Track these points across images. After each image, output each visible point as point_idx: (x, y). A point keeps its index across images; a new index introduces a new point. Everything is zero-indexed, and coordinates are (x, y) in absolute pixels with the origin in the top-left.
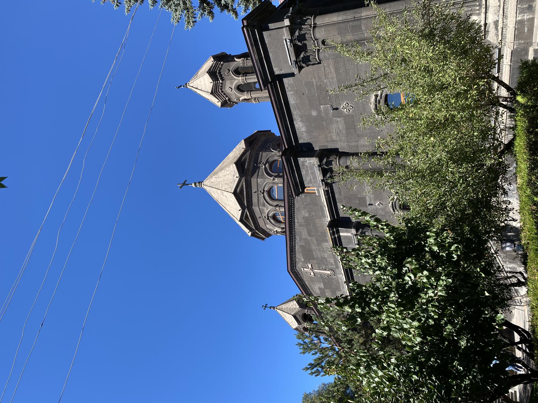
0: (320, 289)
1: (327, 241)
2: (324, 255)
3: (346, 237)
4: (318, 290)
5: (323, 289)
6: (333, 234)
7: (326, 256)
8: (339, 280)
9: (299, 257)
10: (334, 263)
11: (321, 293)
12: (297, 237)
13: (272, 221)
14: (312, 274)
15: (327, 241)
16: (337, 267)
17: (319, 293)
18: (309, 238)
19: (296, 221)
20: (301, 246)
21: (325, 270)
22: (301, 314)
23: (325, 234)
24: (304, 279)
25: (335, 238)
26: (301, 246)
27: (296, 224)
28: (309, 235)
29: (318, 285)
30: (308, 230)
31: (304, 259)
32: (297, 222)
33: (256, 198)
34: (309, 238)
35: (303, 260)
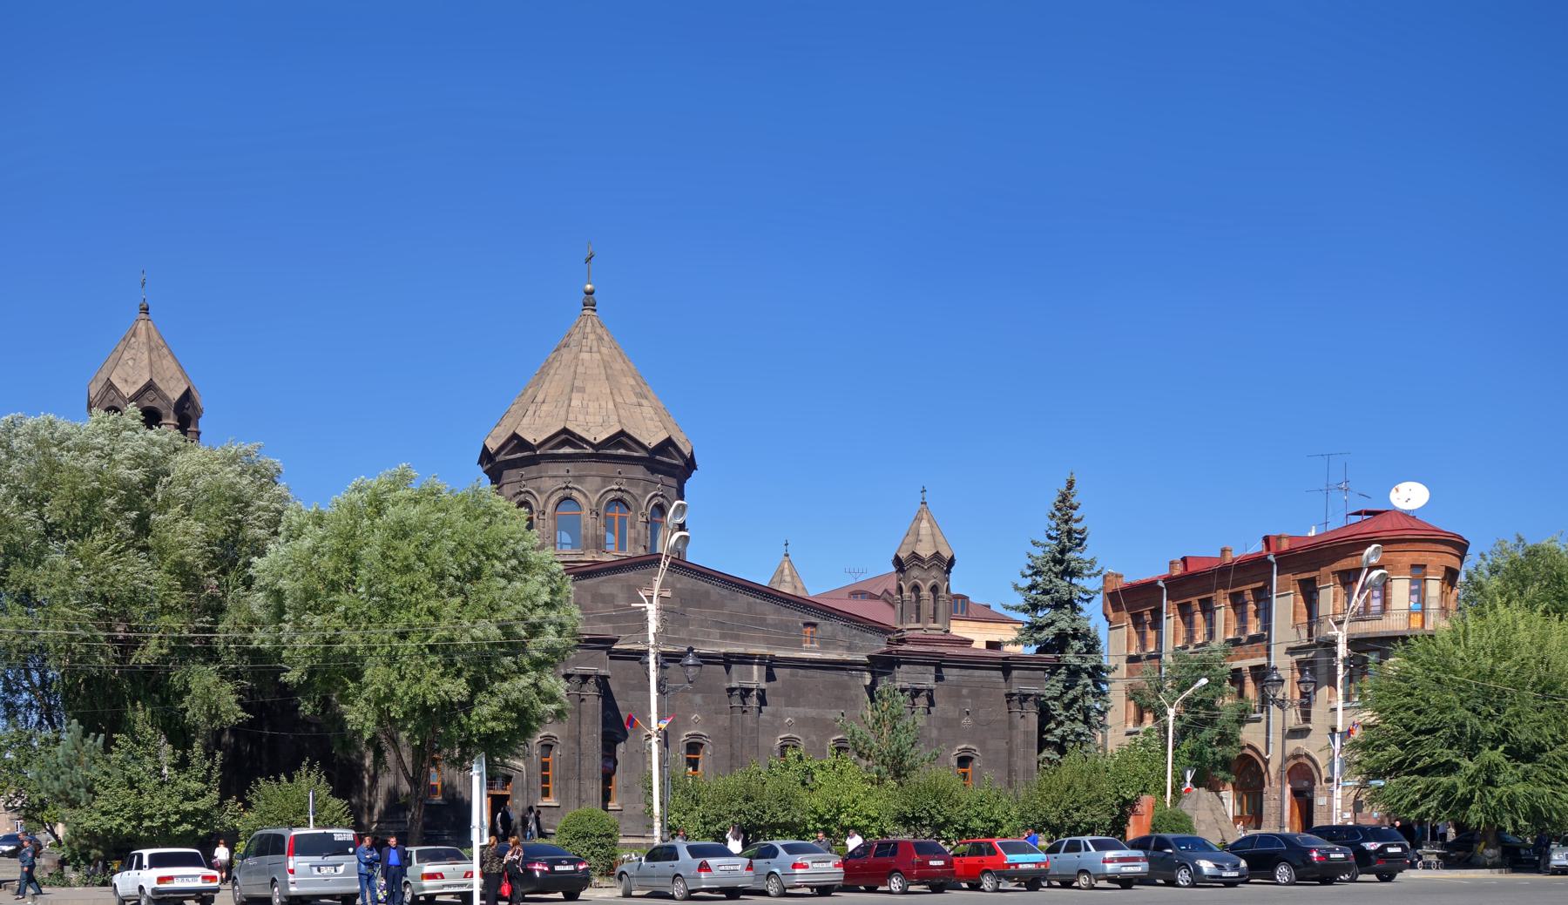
0: (613, 596)
2: (692, 625)
3: (751, 673)
6: (762, 657)
11: (601, 594)
12: (725, 592)
13: (611, 496)
15: (723, 637)
17: (602, 591)
19: (758, 601)
20: (707, 593)
24: (632, 574)
26: (707, 593)
27: (752, 599)
29: (620, 595)
31: (680, 589)
32: (756, 603)
35: (678, 586)
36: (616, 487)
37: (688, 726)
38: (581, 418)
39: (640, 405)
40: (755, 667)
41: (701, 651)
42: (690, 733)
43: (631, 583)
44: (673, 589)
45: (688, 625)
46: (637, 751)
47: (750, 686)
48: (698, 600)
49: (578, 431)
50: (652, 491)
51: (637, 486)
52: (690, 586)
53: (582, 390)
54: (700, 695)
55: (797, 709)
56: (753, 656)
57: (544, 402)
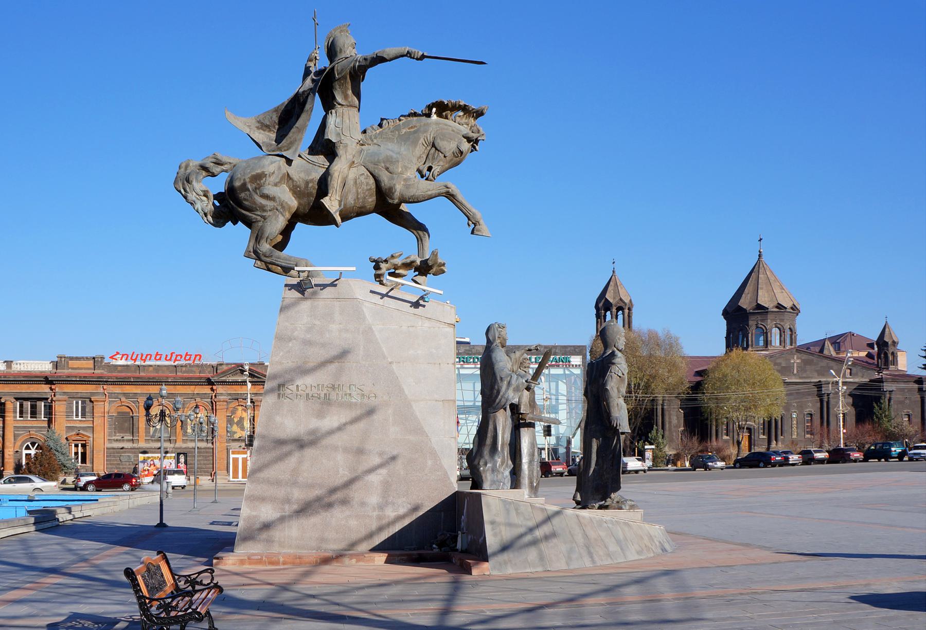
9: (805, 357)
14: (792, 361)
16: (801, 378)
20: (812, 360)
26: (812, 360)
28: (821, 367)
37: (807, 408)
38: (763, 299)
39: (782, 292)
49: (762, 304)
53: (762, 289)
57: (748, 294)
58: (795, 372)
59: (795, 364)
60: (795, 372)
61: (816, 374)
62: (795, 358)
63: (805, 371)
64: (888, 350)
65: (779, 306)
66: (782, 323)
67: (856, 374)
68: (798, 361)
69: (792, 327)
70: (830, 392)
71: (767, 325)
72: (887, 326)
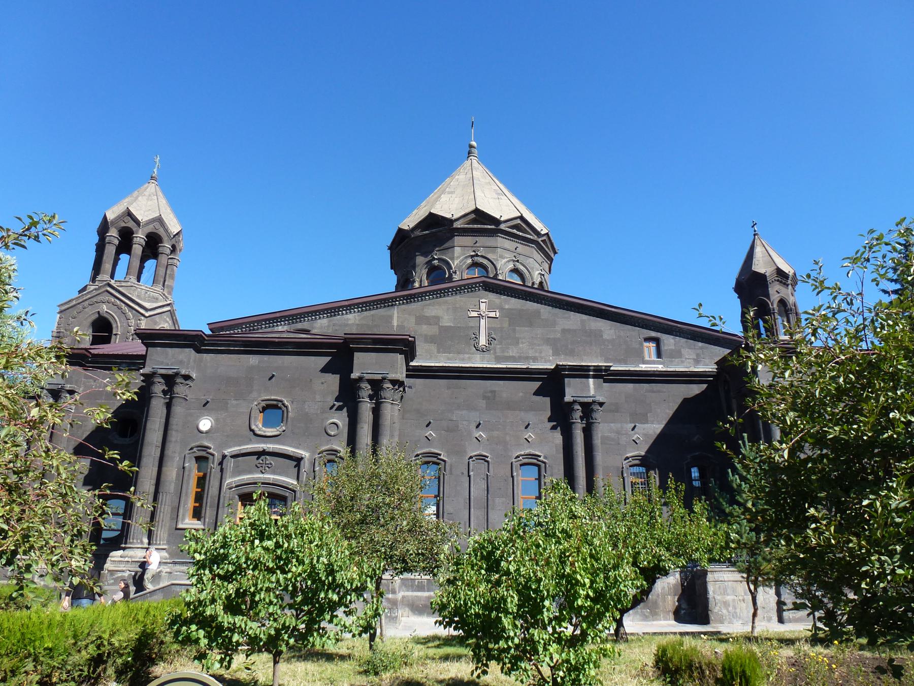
0: (437, 319)
1: (556, 353)
2: (523, 343)
4: (433, 314)
5: (437, 324)
6: (597, 369)
7: (521, 345)
8: (467, 356)
10: (506, 354)
14: (475, 314)
16: (498, 359)
18: (558, 328)
20: (537, 313)
21: (491, 339)
22: (161, 232)
23: (571, 353)
25: (589, 370)
28: (564, 331)
29: (446, 317)
30: (575, 331)
33: (508, 247)
34: (558, 328)
35: (507, 307)
36: (473, 253)
40: (591, 381)
41: (530, 367)
42: (523, 453)
43: (458, 306)
44: (501, 309)
45: (518, 343)
46: (463, 473)
47: (586, 400)
48: (530, 320)
50: (507, 258)
51: (494, 252)
52: (519, 307)
54: (533, 412)
55: (646, 426)
56: (586, 369)
58: (483, 341)
59: (483, 322)
60: (483, 341)
61: (548, 351)
62: (483, 306)
63: (516, 342)
64: (768, 296)
65: (479, 216)
66: (490, 256)
67: (676, 354)
68: (492, 314)
69: (521, 267)
70: (590, 400)
71: (453, 259)
72: (757, 242)
